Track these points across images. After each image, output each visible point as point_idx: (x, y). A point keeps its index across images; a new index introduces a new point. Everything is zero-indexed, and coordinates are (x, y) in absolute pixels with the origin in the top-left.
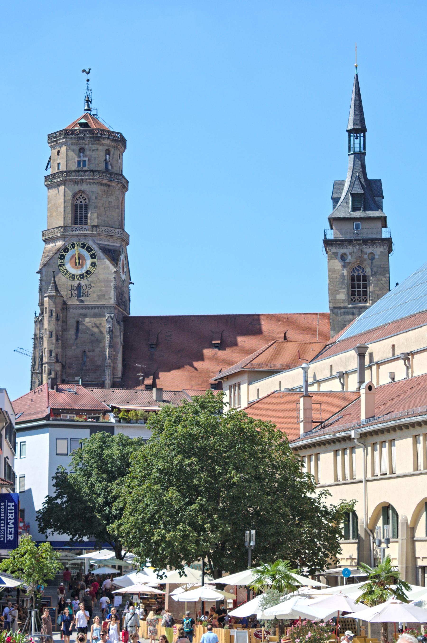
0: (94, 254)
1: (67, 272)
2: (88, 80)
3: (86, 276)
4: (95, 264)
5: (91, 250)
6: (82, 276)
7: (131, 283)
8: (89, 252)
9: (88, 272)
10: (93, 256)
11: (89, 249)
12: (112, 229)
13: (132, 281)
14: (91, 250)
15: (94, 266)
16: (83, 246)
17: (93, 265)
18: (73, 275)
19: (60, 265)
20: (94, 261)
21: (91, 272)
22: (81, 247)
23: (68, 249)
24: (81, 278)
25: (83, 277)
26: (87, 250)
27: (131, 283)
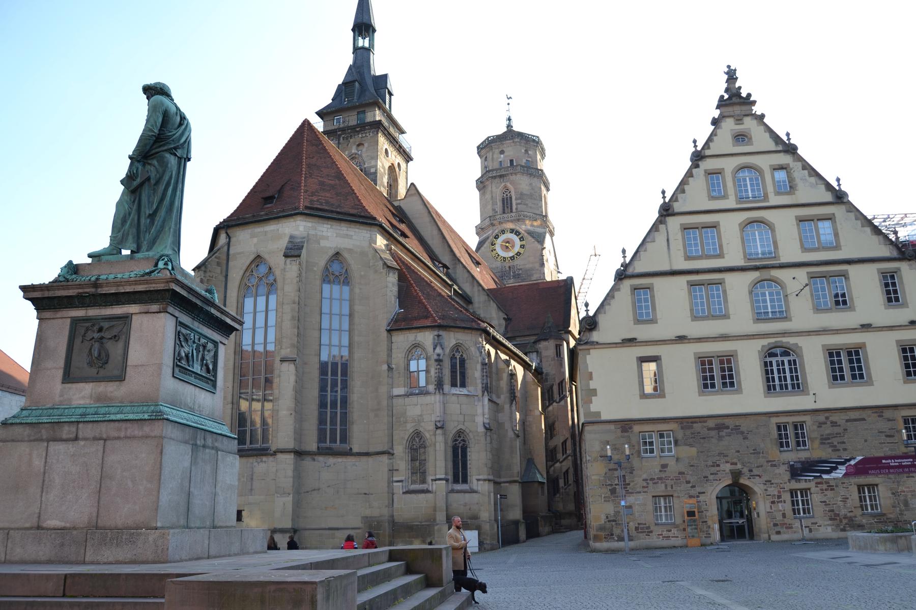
0: (522, 237)
1: (498, 255)
2: (508, 104)
4: (524, 245)
5: (520, 234)
6: (512, 258)
7: (559, 272)
8: (518, 236)
9: (518, 254)
10: (522, 239)
11: (517, 233)
14: (520, 234)
15: (523, 248)
16: (512, 231)
17: (522, 246)
18: (504, 258)
19: (492, 251)
20: (523, 243)
21: (520, 253)
22: (510, 232)
23: (497, 235)
24: (512, 260)
25: (514, 259)
26: (515, 234)
27: (559, 272)
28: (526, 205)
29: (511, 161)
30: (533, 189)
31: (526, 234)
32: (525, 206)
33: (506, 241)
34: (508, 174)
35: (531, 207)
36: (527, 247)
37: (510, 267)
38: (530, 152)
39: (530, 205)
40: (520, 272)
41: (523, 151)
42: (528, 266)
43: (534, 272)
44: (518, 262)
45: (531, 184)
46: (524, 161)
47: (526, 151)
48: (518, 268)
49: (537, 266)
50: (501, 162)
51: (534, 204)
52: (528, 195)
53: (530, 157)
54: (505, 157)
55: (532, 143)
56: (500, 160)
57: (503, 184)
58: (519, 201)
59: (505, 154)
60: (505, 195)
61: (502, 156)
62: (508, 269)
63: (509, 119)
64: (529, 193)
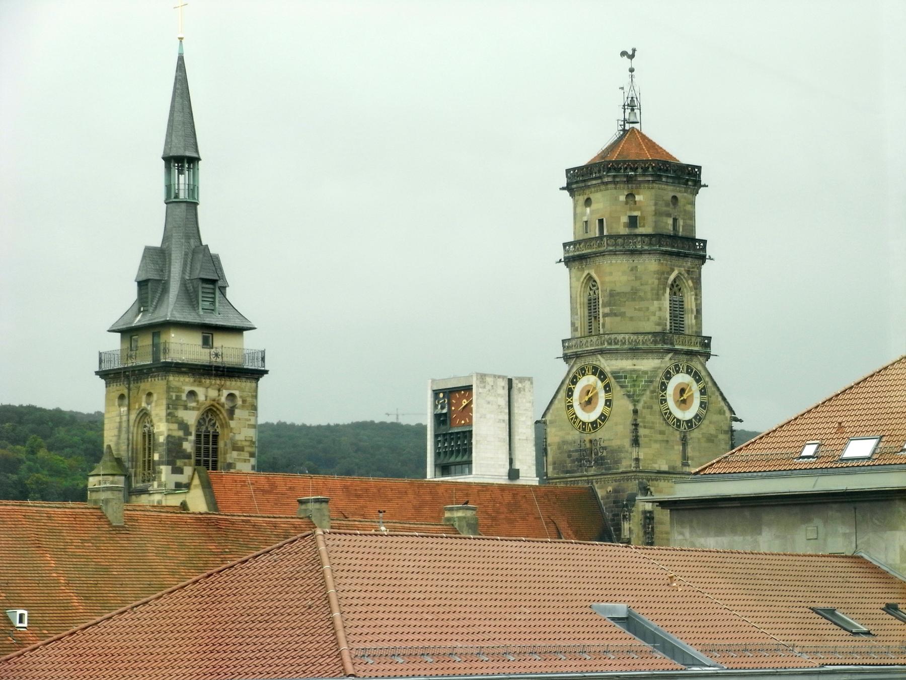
1: (576, 417)
2: (632, 70)
3: (600, 425)
5: (605, 377)
7: (736, 420)
10: (607, 388)
11: (602, 375)
12: (623, 336)
13: (738, 416)
15: (609, 407)
25: (596, 427)
27: (736, 420)
28: (622, 315)
29: (601, 221)
30: (637, 278)
31: (613, 380)
32: (618, 319)
33: (585, 391)
34: (590, 254)
35: (631, 319)
36: (615, 403)
37: (591, 441)
38: (638, 198)
39: (630, 312)
40: (605, 454)
41: (622, 198)
42: (616, 443)
43: (623, 455)
44: (601, 434)
45: (634, 269)
46: (624, 219)
47: (631, 196)
48: (603, 445)
49: (627, 442)
50: (586, 222)
51: (640, 310)
52: (625, 294)
53: (639, 209)
54: (592, 212)
55: (639, 179)
56: (585, 219)
57: (586, 272)
58: (607, 310)
59: (594, 206)
60: (592, 293)
61: (588, 209)
62: (588, 445)
63: (631, 105)
64: (627, 289)
